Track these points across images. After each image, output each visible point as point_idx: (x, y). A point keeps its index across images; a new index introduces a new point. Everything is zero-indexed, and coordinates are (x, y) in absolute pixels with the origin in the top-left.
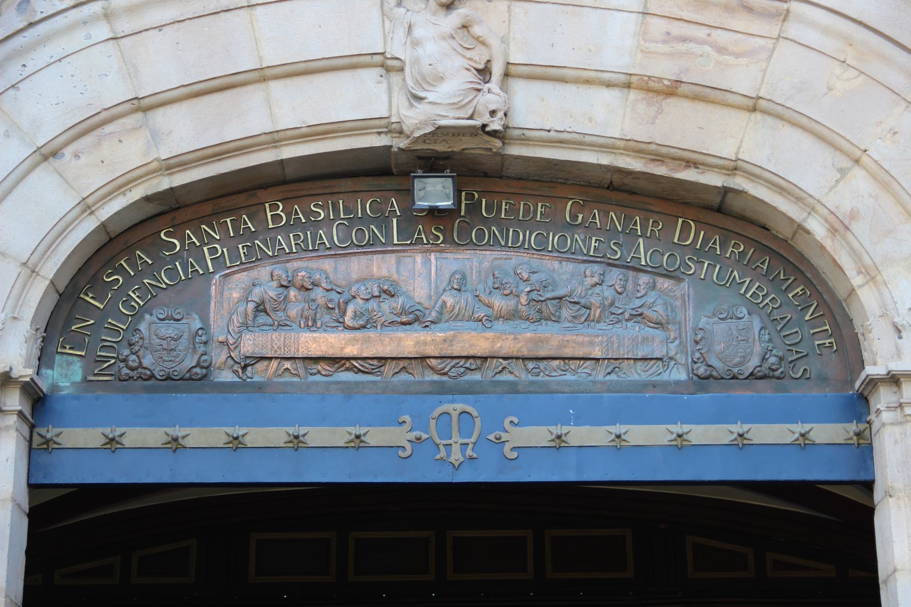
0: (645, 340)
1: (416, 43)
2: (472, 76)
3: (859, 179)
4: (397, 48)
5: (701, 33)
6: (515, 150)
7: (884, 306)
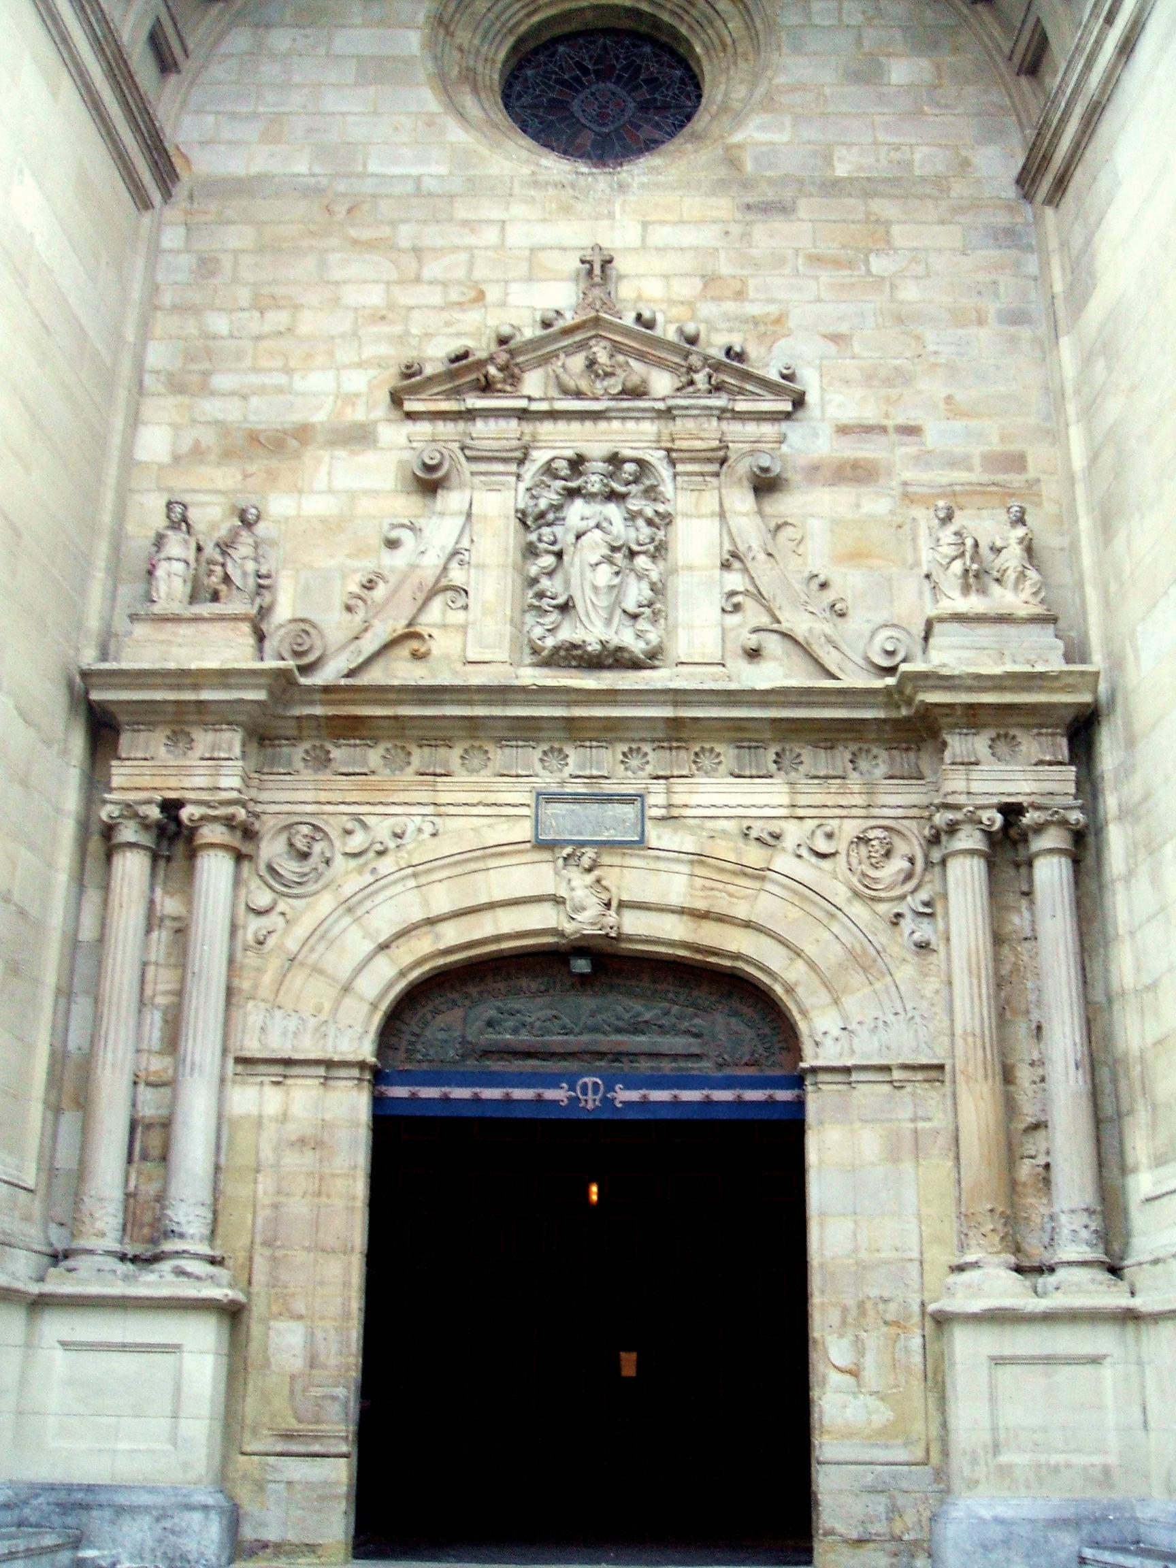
0: (690, 1045)
1: (573, 889)
2: (601, 908)
3: (800, 965)
4: (562, 892)
5: (720, 886)
6: (624, 945)
7: (811, 1031)
